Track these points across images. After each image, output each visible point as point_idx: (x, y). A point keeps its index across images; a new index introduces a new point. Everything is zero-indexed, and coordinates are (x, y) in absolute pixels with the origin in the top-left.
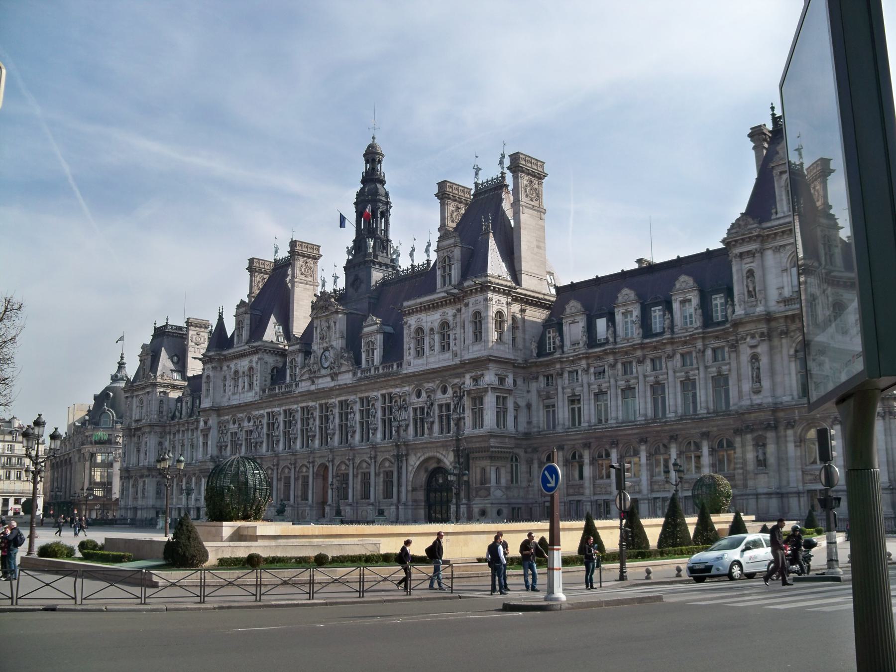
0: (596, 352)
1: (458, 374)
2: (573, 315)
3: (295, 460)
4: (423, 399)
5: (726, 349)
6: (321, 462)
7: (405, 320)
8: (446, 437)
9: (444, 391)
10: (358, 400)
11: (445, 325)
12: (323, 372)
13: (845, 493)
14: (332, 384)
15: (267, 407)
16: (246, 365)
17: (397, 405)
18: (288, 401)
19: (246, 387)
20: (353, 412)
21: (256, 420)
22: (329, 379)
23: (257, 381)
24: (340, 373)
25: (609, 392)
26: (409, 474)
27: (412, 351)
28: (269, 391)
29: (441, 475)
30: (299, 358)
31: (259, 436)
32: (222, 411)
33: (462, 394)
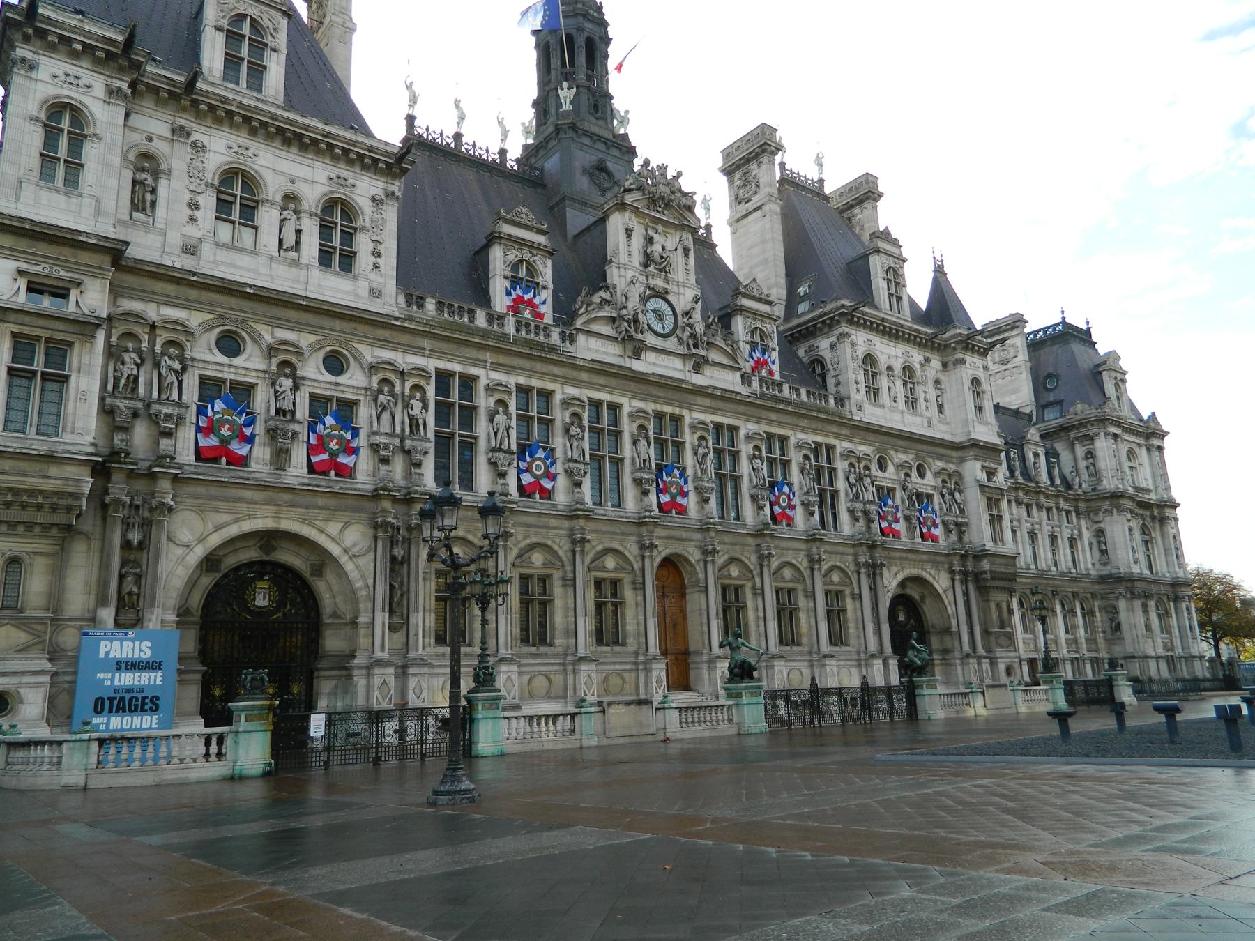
4: (893, 477)
5: (1074, 514)
6: (667, 552)
9: (921, 474)
11: (908, 370)
12: (651, 339)
14: (698, 380)
15: (433, 354)
17: (855, 473)
18: (539, 366)
21: (392, 377)
22: (677, 363)
24: (716, 364)
27: (863, 390)
29: (900, 608)
30: (546, 273)
31: (411, 431)
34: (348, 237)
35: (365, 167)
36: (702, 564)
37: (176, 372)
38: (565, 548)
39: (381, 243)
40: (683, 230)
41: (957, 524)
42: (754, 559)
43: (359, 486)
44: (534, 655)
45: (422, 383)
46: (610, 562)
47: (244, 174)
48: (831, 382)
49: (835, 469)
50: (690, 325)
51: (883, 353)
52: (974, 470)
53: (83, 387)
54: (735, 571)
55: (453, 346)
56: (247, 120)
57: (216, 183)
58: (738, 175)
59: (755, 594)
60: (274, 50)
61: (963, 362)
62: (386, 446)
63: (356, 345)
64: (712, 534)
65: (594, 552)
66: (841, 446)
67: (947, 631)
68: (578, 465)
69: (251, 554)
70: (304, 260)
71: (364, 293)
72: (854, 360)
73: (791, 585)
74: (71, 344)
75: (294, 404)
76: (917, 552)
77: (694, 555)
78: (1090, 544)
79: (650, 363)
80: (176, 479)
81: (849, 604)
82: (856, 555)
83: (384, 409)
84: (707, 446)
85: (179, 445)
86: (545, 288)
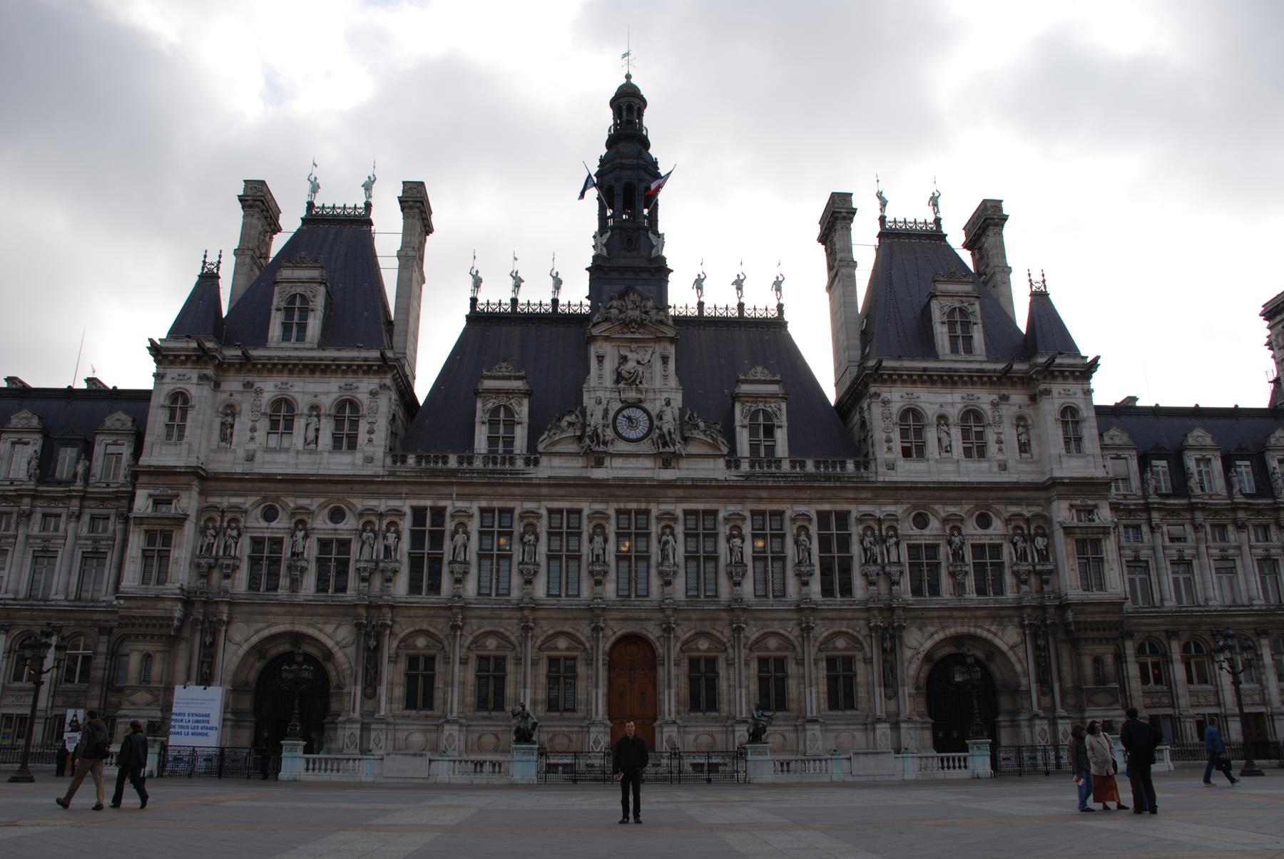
0: (1175, 505)
1: (1017, 499)
2: (1119, 448)
3: (534, 619)
4: (935, 532)
6: (624, 631)
7: (873, 390)
8: (996, 601)
9: (984, 521)
10: (748, 514)
11: (972, 415)
12: (622, 447)
13: (1239, 719)
14: (668, 475)
15: (410, 495)
16: (328, 393)
17: (873, 535)
18: (500, 490)
19: (326, 439)
21: (373, 519)
22: (648, 463)
23: (371, 432)
24: (689, 456)
25: (1195, 562)
26: (906, 664)
27: (897, 445)
28: (419, 462)
30: (523, 410)
31: (386, 557)
32: (212, 485)
33: (1032, 532)
34: (355, 424)
35: (366, 373)
36: (662, 640)
37: (233, 537)
38: (516, 634)
39: (374, 423)
40: (660, 341)
41: (1040, 573)
42: (727, 632)
43: (348, 599)
44: (485, 718)
45: (396, 519)
46: (562, 643)
47: (286, 401)
48: (870, 442)
49: (850, 534)
50: (657, 427)
51: (931, 403)
52: (1062, 512)
53: (176, 556)
54: (703, 645)
55: (426, 487)
56: (285, 365)
57: (268, 411)
58: (828, 243)
59: (727, 664)
60: (312, 310)
62: (365, 569)
63: (351, 500)
64: (669, 612)
65: (545, 635)
66: (855, 510)
67: (1015, 691)
68: (526, 566)
69: (285, 647)
70: (320, 448)
72: (886, 418)
73: (778, 654)
74: (172, 531)
75: (304, 547)
76: (967, 609)
77: (653, 632)
79: (616, 468)
80: (230, 604)
81: (860, 668)
82: (868, 620)
83: (364, 543)
84: (672, 534)
85: (236, 582)
86: (518, 423)
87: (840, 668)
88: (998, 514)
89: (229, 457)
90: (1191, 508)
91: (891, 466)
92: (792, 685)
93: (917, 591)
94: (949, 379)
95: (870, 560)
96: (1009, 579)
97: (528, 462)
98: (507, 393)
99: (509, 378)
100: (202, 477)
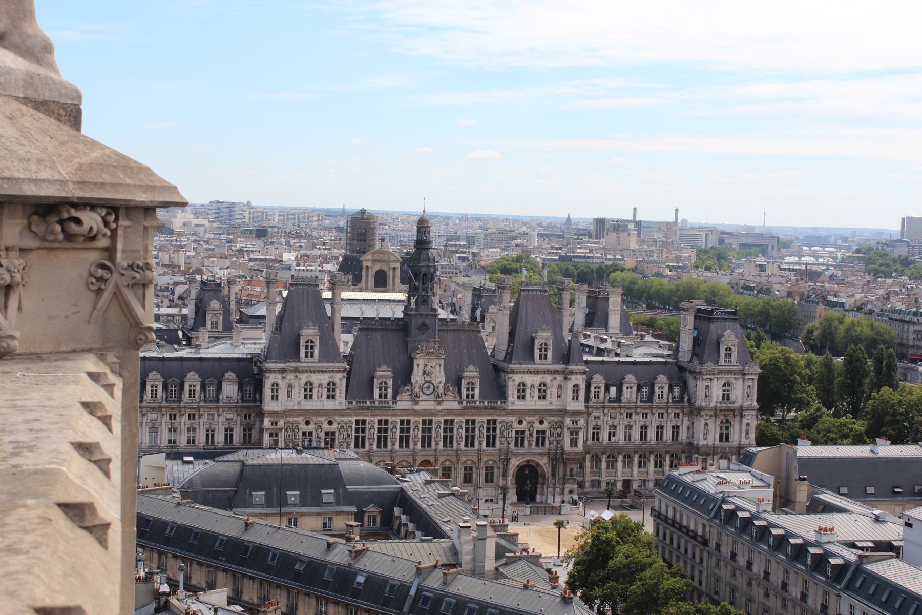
5: (681, 414)
9: (541, 422)
12: (424, 397)
14: (439, 408)
15: (355, 415)
19: (325, 396)
20: (462, 429)
22: (433, 403)
28: (357, 403)
34: (334, 390)
42: (455, 459)
54: (447, 463)
61: (570, 379)
66: (499, 419)
67: (543, 476)
71: (337, 404)
72: (513, 386)
78: (688, 429)
81: (496, 470)
82: (500, 455)
87: (489, 469)
88: (546, 420)
89: (292, 403)
90: (620, 407)
91: (513, 403)
92: (474, 476)
93: (516, 445)
94: (537, 372)
95: (502, 436)
96: (547, 442)
97: (393, 403)
98: (386, 377)
99: (385, 371)
100: (286, 413)
